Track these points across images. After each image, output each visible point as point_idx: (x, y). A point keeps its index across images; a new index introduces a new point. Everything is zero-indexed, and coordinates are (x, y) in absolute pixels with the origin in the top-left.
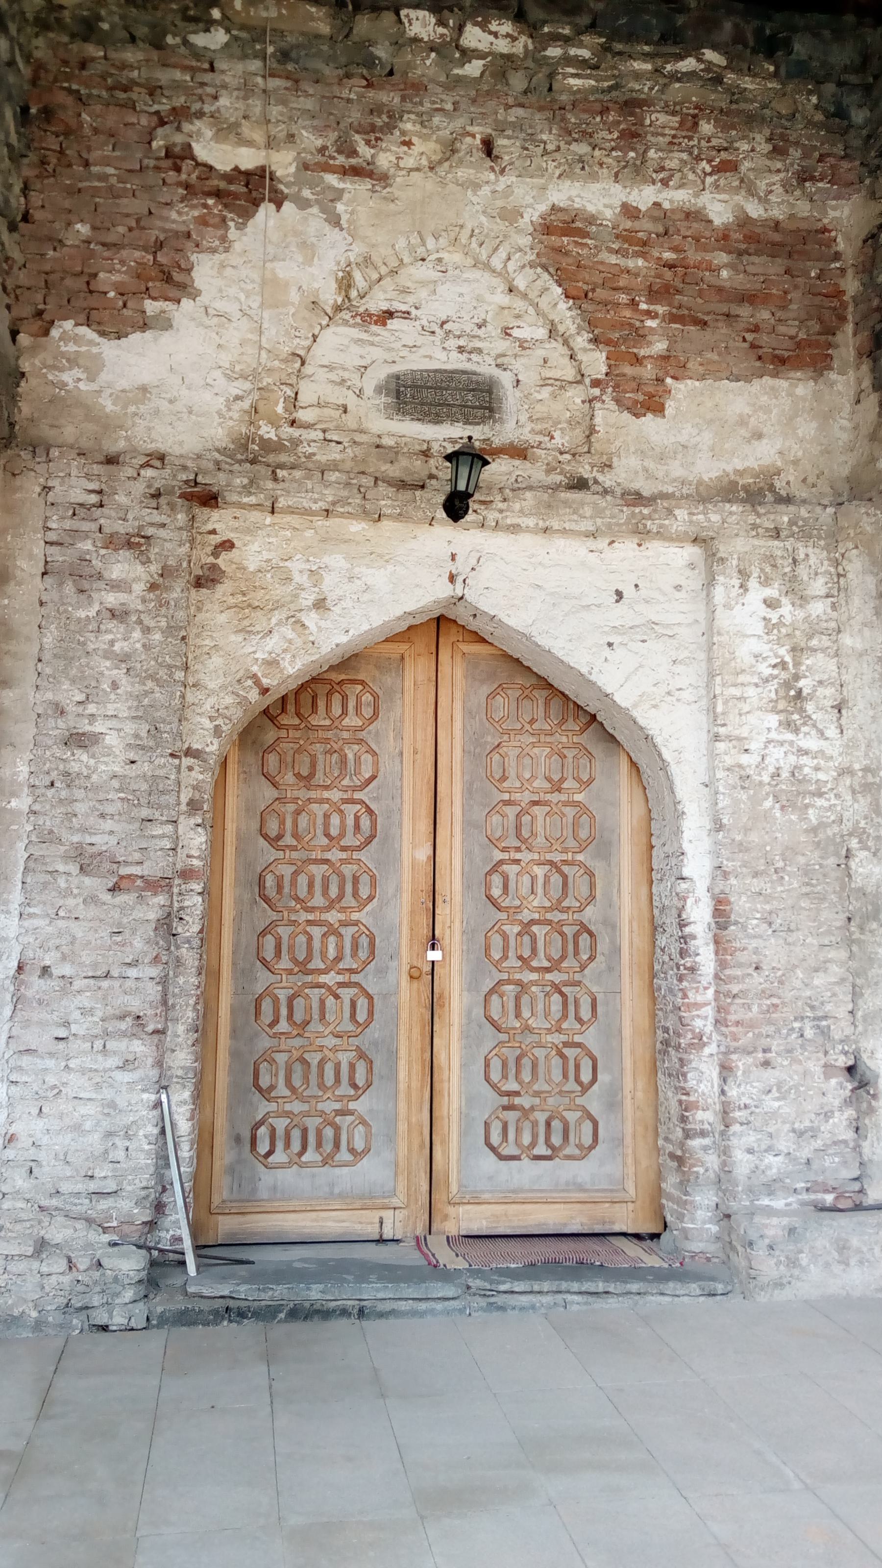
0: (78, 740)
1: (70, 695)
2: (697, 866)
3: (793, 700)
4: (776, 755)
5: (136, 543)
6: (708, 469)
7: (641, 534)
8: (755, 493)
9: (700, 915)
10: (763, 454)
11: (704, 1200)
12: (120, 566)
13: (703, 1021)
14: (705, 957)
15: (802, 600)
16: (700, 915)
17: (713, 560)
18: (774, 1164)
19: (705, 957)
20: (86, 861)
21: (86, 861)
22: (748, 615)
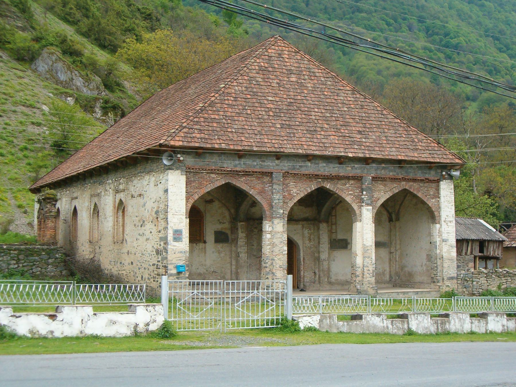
0: (253, 245)
1: (252, 242)
2: (302, 255)
3: (310, 240)
4: (309, 245)
5: (256, 228)
6: (302, 217)
7: (297, 224)
8: (306, 219)
9: (302, 259)
10: (307, 215)
11: (302, 284)
12: (255, 230)
13: (302, 269)
14: (302, 263)
15: (310, 229)
16: (302, 259)
17: (303, 227)
18: (308, 280)
19: (302, 263)
20: (254, 255)
21: (254, 255)
22: (306, 232)
